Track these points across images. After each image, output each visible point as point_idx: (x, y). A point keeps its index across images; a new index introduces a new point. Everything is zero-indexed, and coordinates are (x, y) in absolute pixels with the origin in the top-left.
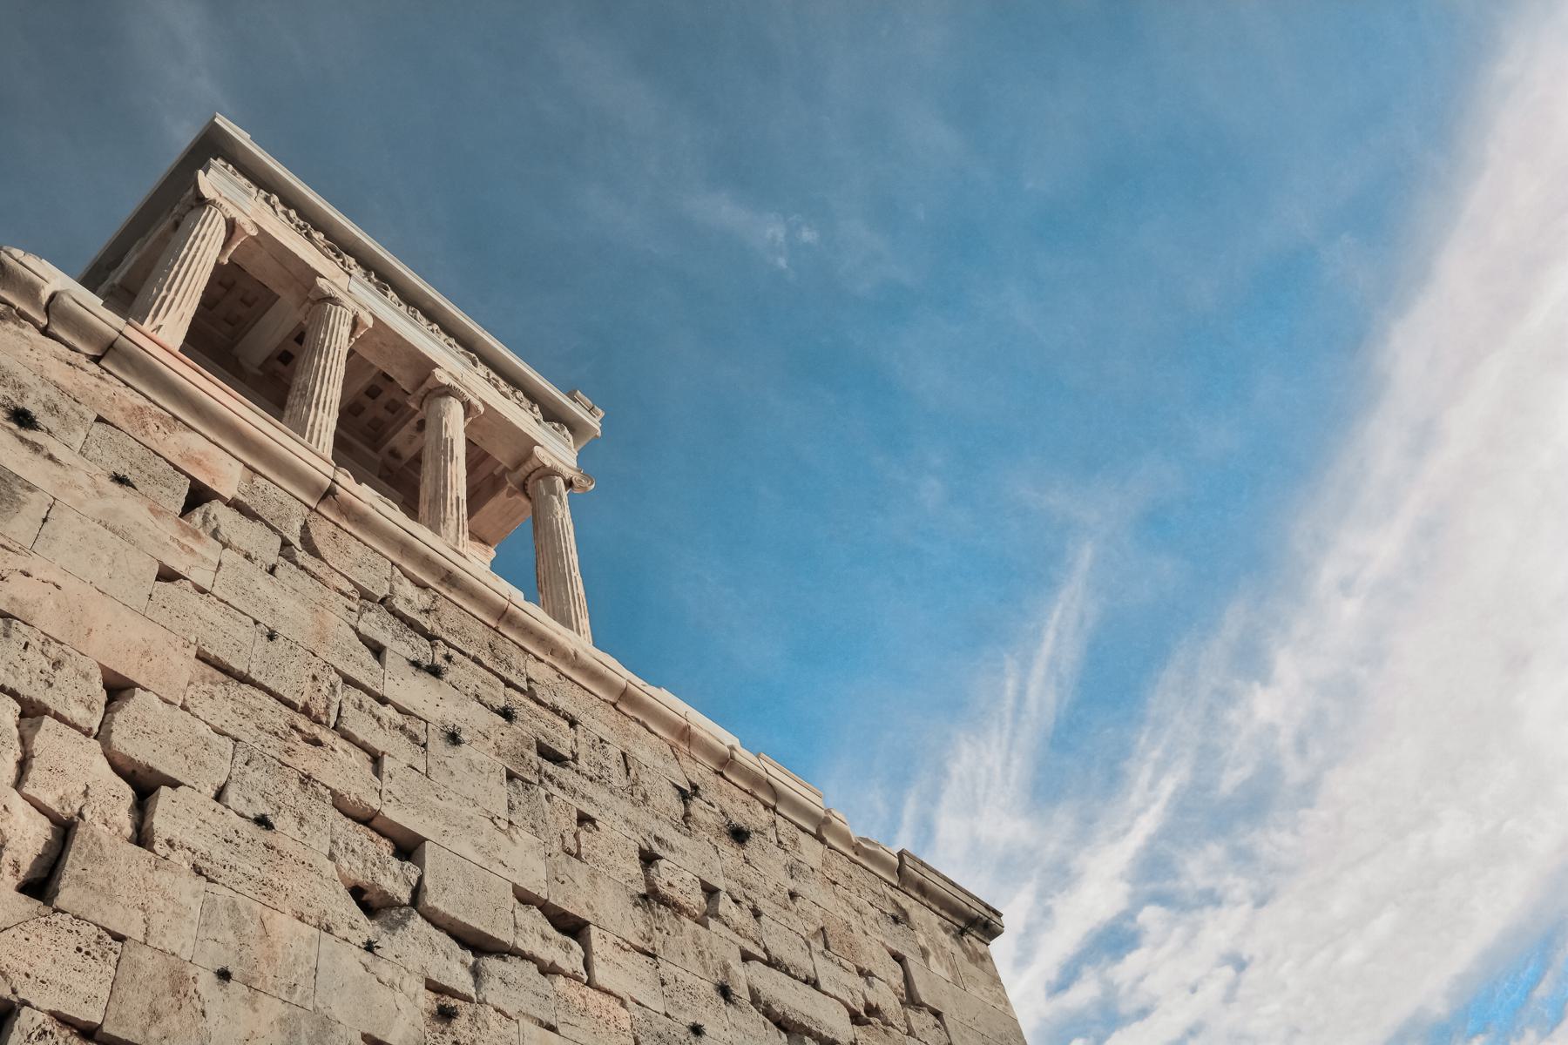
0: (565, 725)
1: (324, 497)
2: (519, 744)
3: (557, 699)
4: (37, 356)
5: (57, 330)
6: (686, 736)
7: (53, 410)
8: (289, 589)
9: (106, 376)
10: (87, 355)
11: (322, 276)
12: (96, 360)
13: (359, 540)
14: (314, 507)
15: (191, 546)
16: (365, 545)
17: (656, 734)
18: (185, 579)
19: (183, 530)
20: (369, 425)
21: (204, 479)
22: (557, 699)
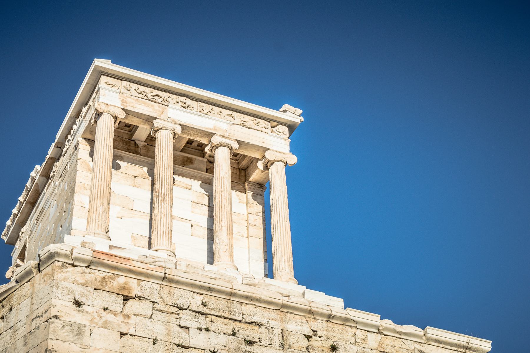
0: (256, 328)
1: (163, 279)
2: (238, 344)
3: (254, 318)
4: (74, 277)
5: (75, 263)
6: (311, 313)
7: (83, 295)
8: (157, 321)
9: (93, 271)
10: (86, 267)
11: (156, 118)
12: (88, 267)
13: (177, 288)
14: (160, 283)
15: (127, 321)
16: (180, 289)
17: (299, 315)
18: (128, 334)
19: (124, 317)
20: (197, 146)
21: (126, 294)
22: (254, 318)
